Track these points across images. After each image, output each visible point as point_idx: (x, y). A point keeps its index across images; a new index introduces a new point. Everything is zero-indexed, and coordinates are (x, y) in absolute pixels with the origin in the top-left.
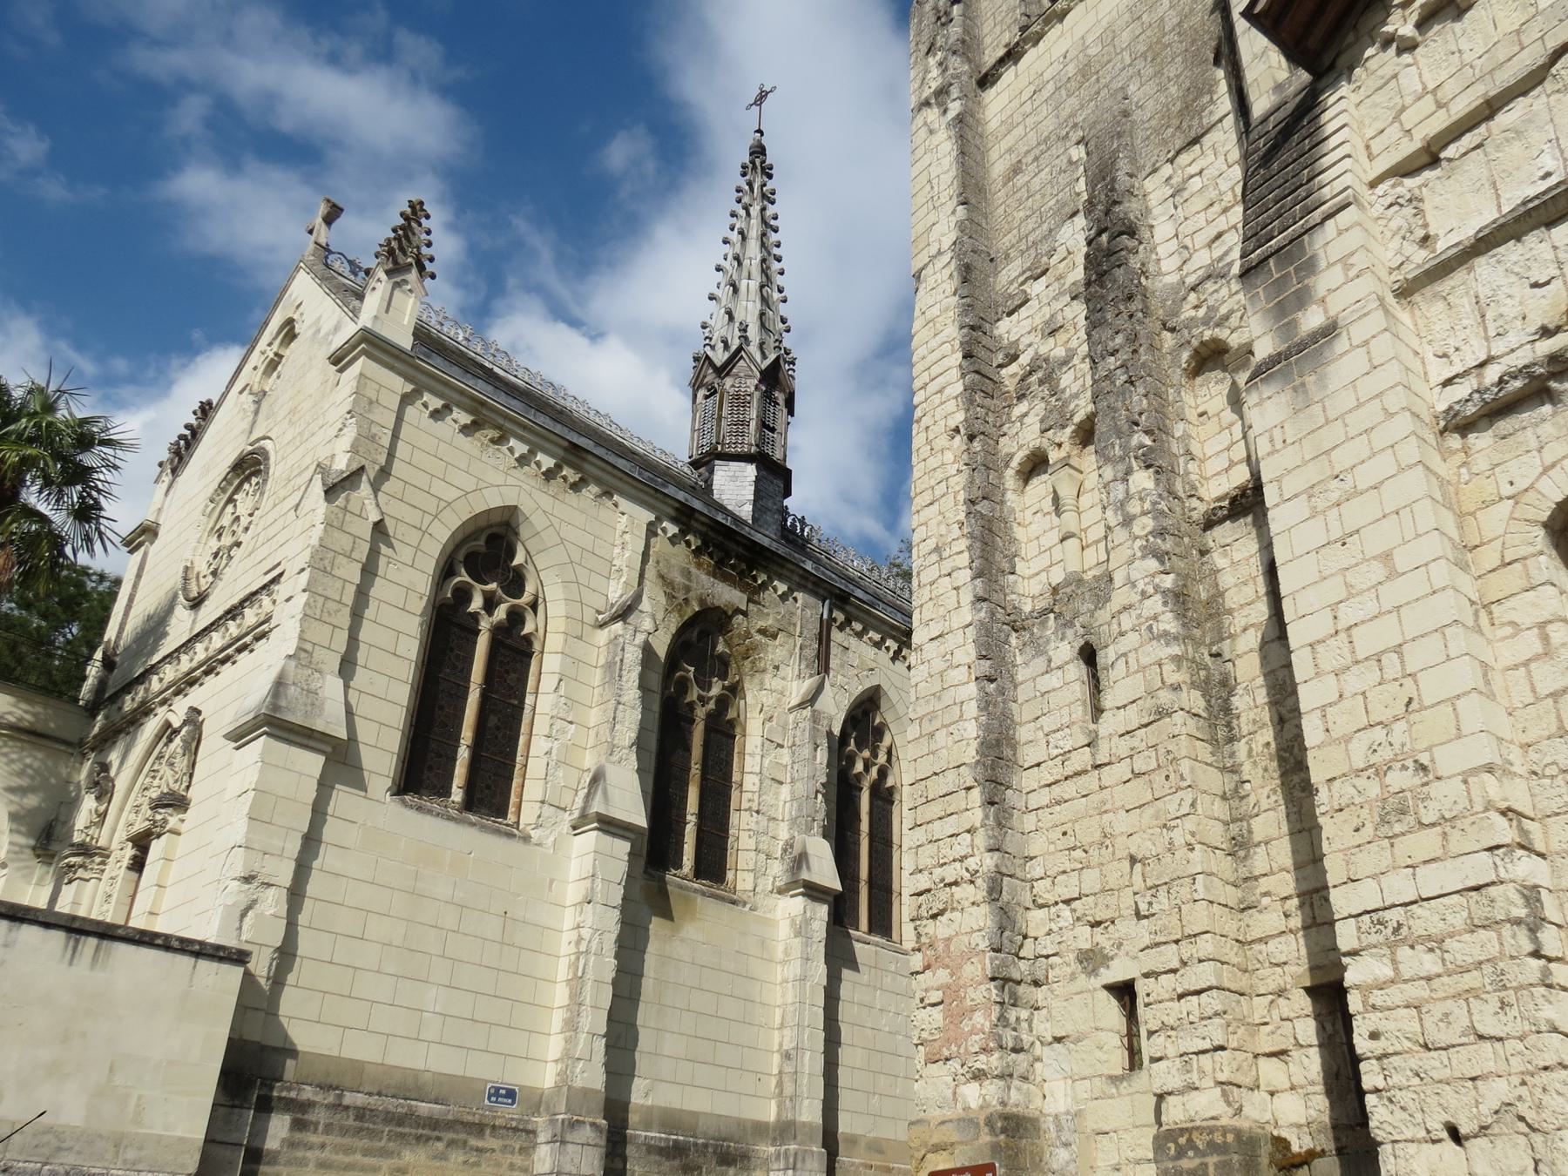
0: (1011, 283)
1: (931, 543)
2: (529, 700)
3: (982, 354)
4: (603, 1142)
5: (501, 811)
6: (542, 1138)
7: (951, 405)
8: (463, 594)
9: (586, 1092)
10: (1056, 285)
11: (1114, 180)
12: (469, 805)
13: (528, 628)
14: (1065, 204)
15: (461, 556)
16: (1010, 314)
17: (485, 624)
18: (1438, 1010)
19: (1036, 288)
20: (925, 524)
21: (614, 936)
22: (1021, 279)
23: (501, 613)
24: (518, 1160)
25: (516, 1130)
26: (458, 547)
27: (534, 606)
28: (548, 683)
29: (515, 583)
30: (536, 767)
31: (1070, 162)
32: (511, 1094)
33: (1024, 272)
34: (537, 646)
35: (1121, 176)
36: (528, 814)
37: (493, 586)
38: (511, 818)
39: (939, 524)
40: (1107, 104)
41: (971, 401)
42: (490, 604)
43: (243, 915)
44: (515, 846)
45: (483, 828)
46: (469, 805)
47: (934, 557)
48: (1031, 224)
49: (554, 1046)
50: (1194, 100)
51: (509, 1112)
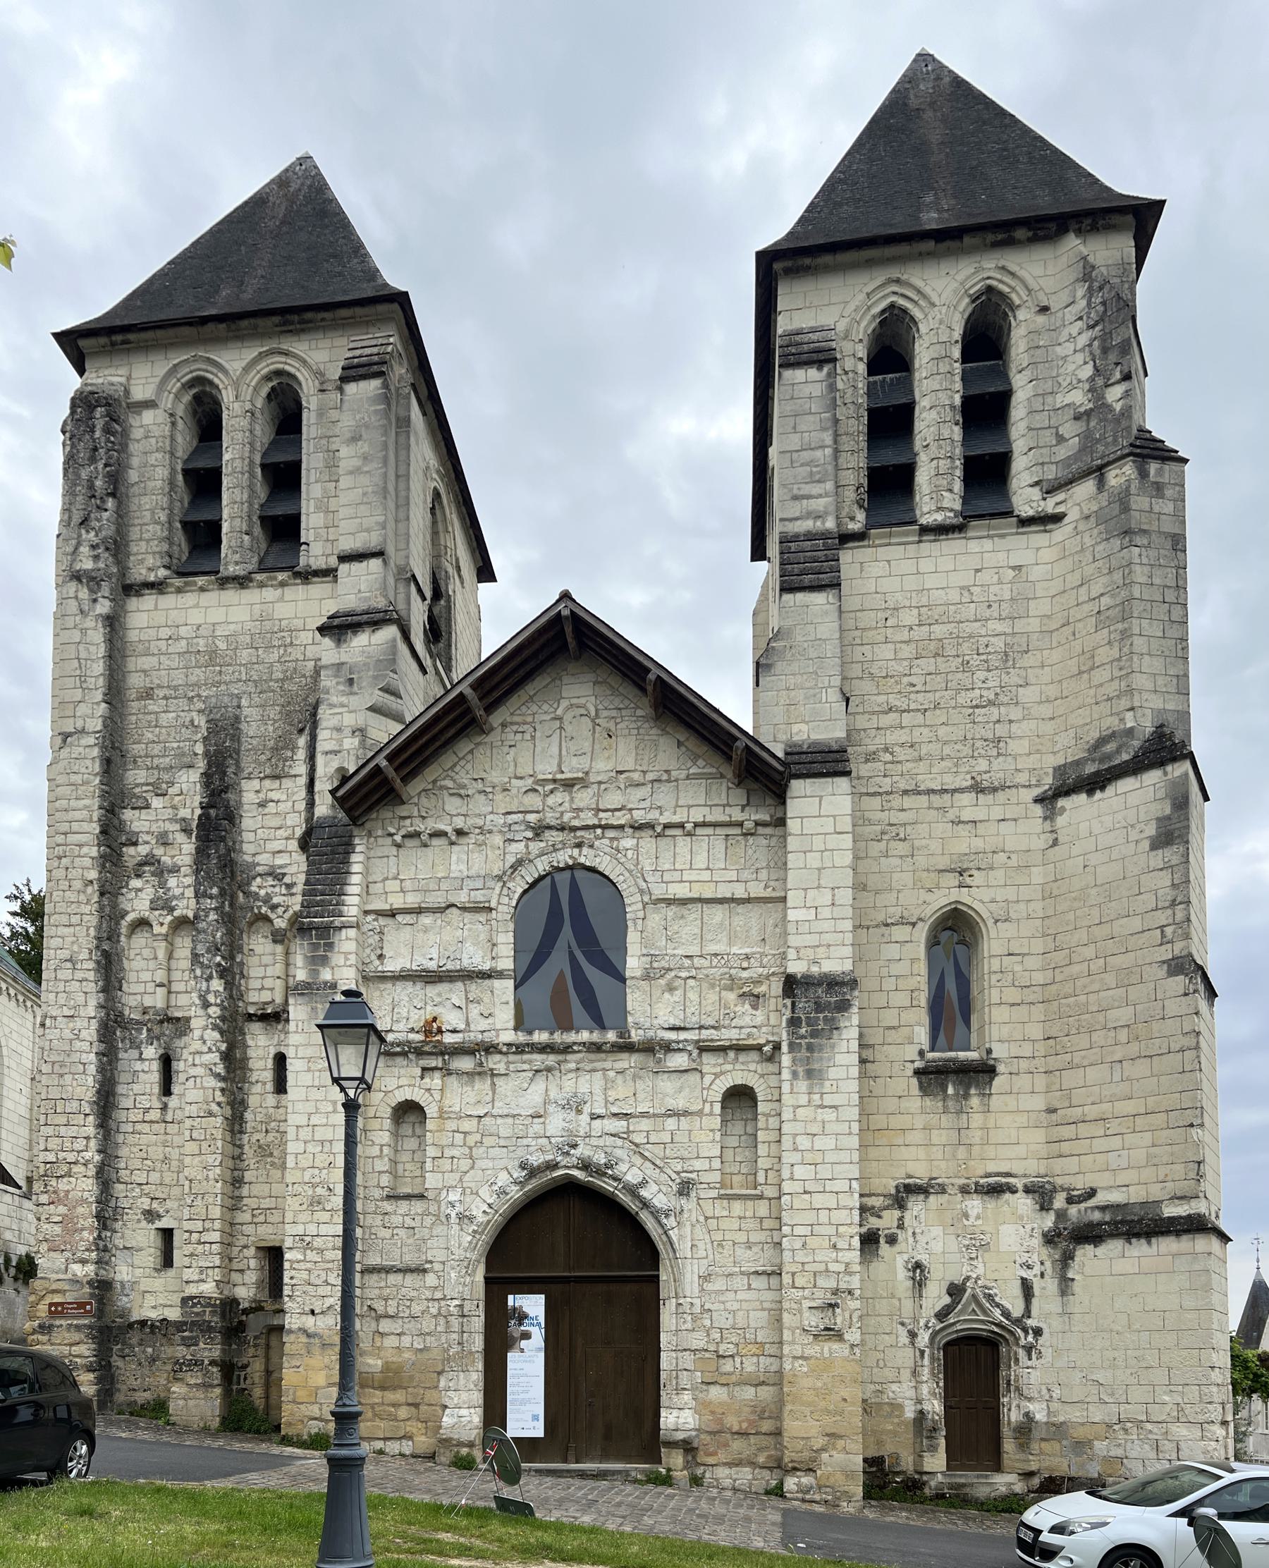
0: (137, 785)
1: (65, 954)
3: (113, 832)
7: (87, 862)
10: (170, 810)
11: (224, 773)
14: (183, 754)
16: (133, 808)
18: (316, 1273)
19: (156, 802)
20: (63, 938)
22: (145, 788)
31: (192, 721)
33: (147, 784)
35: (230, 770)
39: (73, 943)
40: (226, 699)
41: (103, 866)
47: (69, 965)
48: (157, 749)
50: (282, 749)
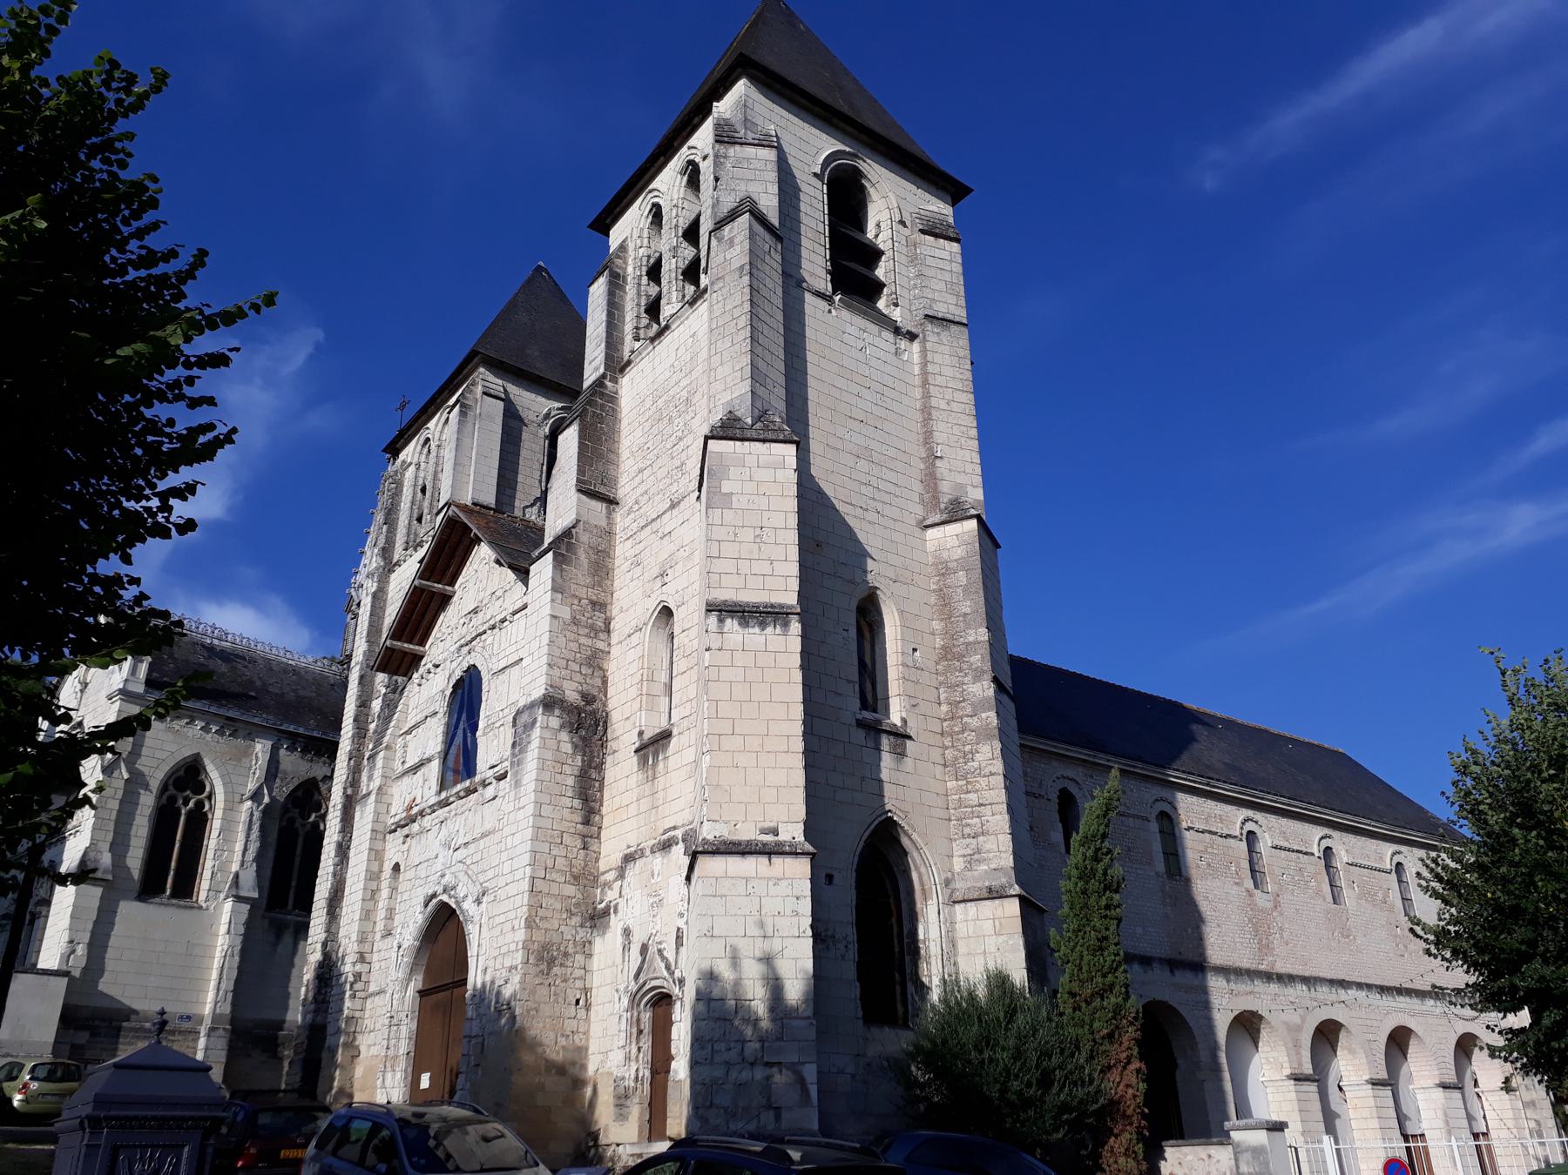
2: (205, 843)
4: (228, 1035)
5: (190, 895)
6: (202, 1035)
8: (172, 799)
9: (221, 1015)
12: (174, 895)
13: (207, 807)
15: (171, 782)
17: (183, 812)
21: (239, 947)
23: (191, 804)
24: (191, 1044)
25: (190, 1032)
26: (170, 777)
27: (209, 797)
28: (215, 833)
29: (200, 788)
30: (207, 874)
32: (189, 1018)
34: (210, 816)
36: (202, 896)
37: (188, 792)
38: (194, 899)
42: (186, 803)
43: (69, 956)
44: (195, 912)
45: (179, 906)
46: (174, 895)
49: (211, 996)
51: (186, 1025)
